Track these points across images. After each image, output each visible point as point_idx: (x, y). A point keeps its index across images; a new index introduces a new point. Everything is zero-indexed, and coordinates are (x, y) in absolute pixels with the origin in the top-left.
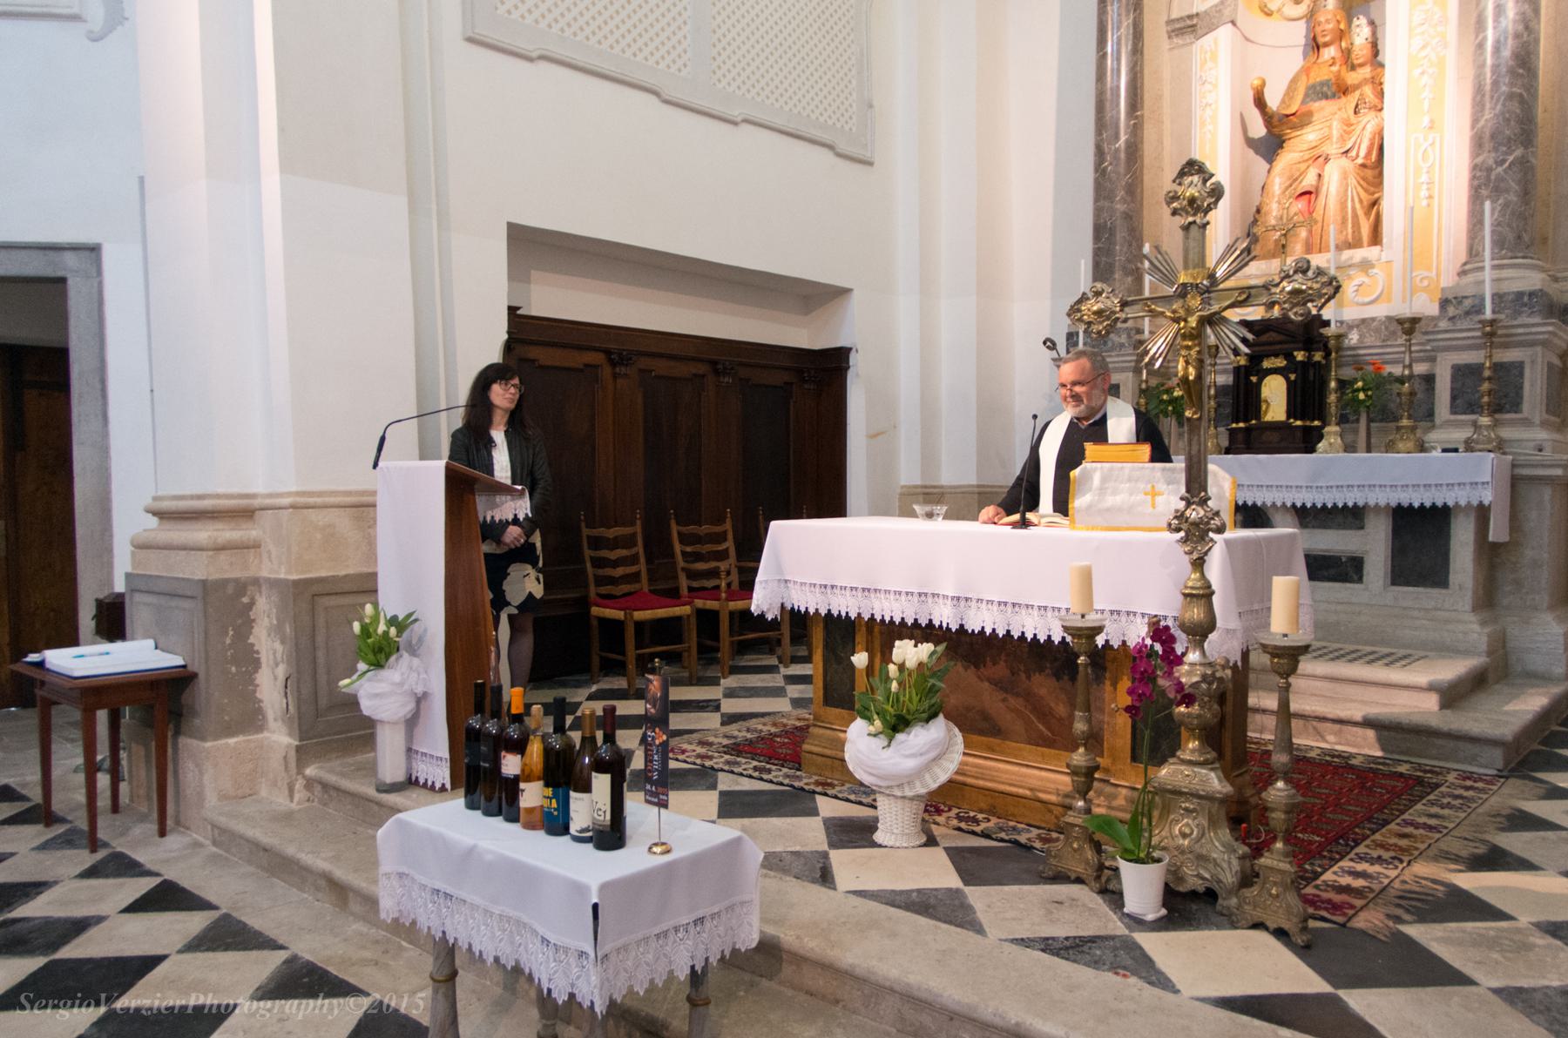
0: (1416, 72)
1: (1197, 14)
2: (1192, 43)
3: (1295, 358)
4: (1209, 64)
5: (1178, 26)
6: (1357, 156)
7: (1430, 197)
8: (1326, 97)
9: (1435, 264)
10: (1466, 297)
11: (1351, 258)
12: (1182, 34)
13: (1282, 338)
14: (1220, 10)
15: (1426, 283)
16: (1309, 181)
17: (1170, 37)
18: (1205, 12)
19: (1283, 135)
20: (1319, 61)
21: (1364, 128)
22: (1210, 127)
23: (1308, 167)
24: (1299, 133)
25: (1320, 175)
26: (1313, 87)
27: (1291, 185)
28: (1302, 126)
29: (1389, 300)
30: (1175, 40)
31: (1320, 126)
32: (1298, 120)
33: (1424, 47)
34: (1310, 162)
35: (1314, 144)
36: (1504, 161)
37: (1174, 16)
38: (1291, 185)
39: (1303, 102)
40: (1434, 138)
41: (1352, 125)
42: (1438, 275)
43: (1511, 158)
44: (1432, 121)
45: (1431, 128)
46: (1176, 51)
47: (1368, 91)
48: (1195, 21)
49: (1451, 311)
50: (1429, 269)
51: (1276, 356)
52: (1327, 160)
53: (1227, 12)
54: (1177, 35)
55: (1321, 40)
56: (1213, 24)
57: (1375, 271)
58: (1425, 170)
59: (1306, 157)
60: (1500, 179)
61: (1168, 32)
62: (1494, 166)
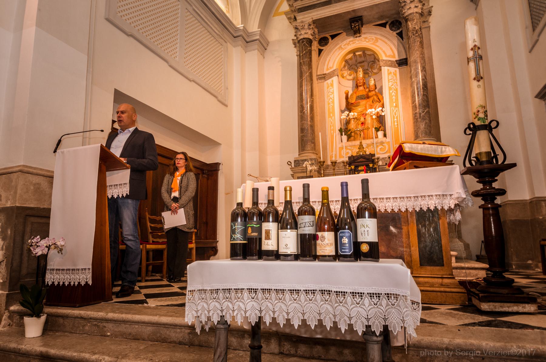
0: (391, 91)
3: (369, 166)
4: (330, 87)
5: (320, 77)
8: (363, 99)
13: (365, 160)
17: (317, 80)
18: (328, 73)
22: (332, 104)
25: (365, 119)
26: (358, 96)
28: (357, 106)
31: (363, 106)
32: (356, 105)
33: (392, 85)
35: (361, 111)
36: (424, 112)
37: (318, 74)
39: (356, 100)
43: (426, 111)
44: (396, 105)
46: (319, 84)
47: (376, 98)
51: (363, 166)
53: (336, 73)
55: (359, 84)
59: (360, 114)
60: (424, 116)
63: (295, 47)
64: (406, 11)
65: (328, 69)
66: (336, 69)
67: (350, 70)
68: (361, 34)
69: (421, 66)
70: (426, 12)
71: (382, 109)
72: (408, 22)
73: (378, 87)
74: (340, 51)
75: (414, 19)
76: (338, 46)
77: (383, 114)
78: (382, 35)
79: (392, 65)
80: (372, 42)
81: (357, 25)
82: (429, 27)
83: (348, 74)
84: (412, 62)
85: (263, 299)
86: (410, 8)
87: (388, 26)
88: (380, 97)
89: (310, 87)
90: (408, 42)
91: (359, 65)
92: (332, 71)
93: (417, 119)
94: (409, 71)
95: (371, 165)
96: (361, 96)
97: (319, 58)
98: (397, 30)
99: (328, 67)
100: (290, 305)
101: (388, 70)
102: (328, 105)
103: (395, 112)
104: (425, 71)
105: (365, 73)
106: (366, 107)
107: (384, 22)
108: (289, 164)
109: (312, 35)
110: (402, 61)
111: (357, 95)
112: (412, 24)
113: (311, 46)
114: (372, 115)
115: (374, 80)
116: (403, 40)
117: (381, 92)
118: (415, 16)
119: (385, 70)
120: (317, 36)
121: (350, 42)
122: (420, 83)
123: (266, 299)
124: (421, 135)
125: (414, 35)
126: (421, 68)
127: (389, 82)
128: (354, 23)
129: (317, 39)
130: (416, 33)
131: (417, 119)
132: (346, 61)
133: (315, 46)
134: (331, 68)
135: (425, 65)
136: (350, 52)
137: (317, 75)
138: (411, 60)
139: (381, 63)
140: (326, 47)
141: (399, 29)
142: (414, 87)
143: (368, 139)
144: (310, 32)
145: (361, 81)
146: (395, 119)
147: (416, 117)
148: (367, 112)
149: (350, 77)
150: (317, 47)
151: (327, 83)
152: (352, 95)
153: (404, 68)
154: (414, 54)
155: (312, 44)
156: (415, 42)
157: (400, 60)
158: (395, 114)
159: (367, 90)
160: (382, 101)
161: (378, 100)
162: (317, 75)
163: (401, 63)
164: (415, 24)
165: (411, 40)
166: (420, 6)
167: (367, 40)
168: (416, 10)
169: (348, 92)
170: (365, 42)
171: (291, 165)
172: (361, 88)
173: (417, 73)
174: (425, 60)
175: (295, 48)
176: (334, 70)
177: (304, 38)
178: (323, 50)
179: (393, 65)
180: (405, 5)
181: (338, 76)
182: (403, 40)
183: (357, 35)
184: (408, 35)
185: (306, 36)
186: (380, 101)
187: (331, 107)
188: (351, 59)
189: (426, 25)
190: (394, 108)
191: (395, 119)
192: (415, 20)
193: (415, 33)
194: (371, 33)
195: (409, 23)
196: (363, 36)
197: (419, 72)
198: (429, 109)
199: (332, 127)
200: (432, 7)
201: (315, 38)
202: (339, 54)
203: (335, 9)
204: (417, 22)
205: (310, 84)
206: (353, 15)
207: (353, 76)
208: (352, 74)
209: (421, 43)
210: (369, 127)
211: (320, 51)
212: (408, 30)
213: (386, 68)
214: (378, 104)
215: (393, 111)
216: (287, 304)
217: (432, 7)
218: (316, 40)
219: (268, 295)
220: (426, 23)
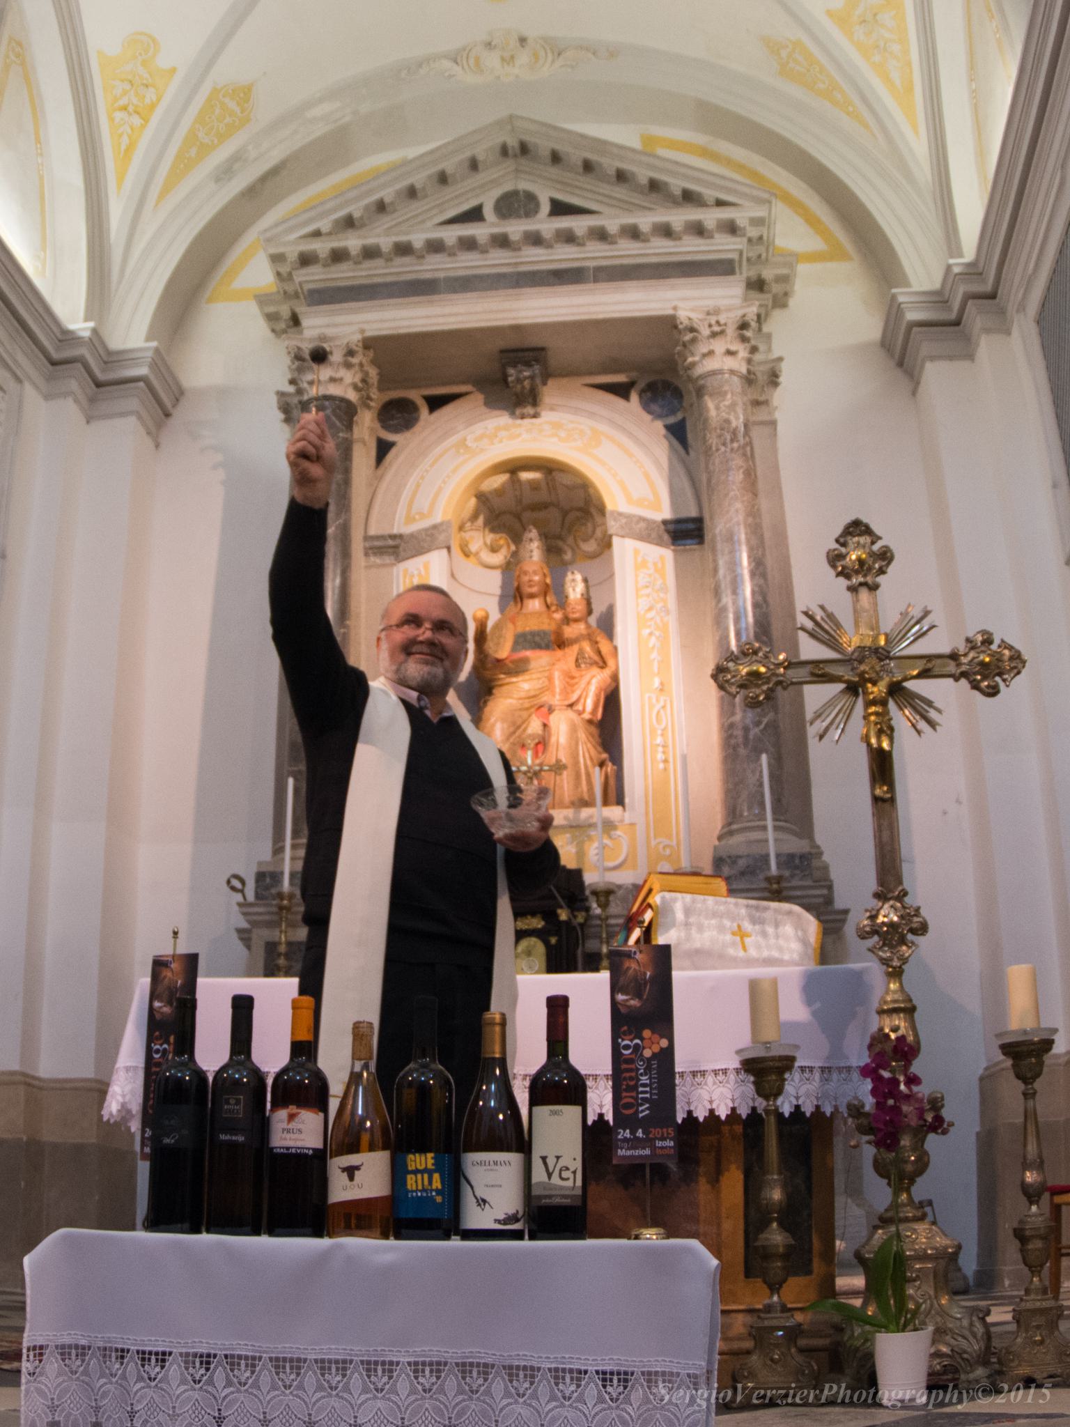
0: (646, 632)
1: (400, 536)
2: (393, 565)
3: (556, 916)
6: (584, 710)
7: (666, 761)
9: (674, 832)
10: (740, 857)
11: (591, 817)
15: (668, 852)
16: (535, 726)
17: (366, 554)
18: (412, 536)
20: (524, 611)
21: (589, 683)
23: (530, 716)
24: (514, 680)
25: (545, 725)
27: (514, 733)
29: (634, 867)
30: (372, 559)
33: (650, 609)
34: (533, 710)
35: (532, 693)
37: (372, 531)
38: (514, 733)
40: (665, 701)
42: (678, 844)
43: (765, 720)
44: (662, 684)
45: (662, 690)
48: (397, 542)
49: (726, 870)
50: (669, 837)
51: (533, 914)
52: (551, 710)
53: (442, 537)
54: (375, 554)
55: (527, 590)
57: (618, 833)
58: (659, 732)
59: (527, 705)
61: (365, 548)
62: (751, 726)
64: (697, 358)
65: (410, 519)
66: (441, 524)
67: (493, 530)
68: (539, 409)
69: (749, 557)
70: (761, 371)
72: (706, 398)
73: (597, 608)
75: (726, 393)
76: (453, 439)
78: (611, 422)
79: (649, 535)
81: (526, 378)
82: (773, 424)
83: (485, 544)
84: (719, 538)
85: (274, 1387)
86: (711, 353)
87: (634, 397)
88: (605, 647)
89: (338, 581)
90: (707, 467)
91: (527, 515)
92: (426, 530)
93: (735, 748)
94: (711, 566)
95: (563, 915)
96: (533, 634)
97: (380, 471)
98: (667, 416)
99: (414, 511)
100: (361, 1405)
101: (636, 552)
103: (658, 712)
104: (764, 575)
105: (553, 550)
107: (621, 378)
108: (233, 889)
109: (356, 387)
110: (684, 526)
111: (520, 630)
112: (717, 408)
113: (349, 426)
115: (585, 580)
116: (688, 453)
117: (607, 625)
118: (727, 381)
119: (626, 551)
120: (374, 393)
121: (498, 429)
122: (746, 617)
123: (285, 1387)
124: (750, 808)
125: (724, 444)
126: (749, 563)
127: (637, 596)
128: (515, 367)
129: (372, 404)
130: (732, 441)
131: (735, 748)
132: (482, 498)
133: (366, 426)
134: (423, 516)
135: (764, 555)
136: (498, 468)
137: (367, 538)
138: (717, 528)
139: (612, 526)
140: (408, 434)
141: (673, 412)
142: (727, 629)
144: (349, 377)
145: (536, 578)
147: (733, 741)
149: (495, 555)
150: (372, 429)
151: (406, 571)
152: (498, 626)
153: (691, 546)
154: (728, 512)
155: (355, 419)
156: (728, 470)
157: (678, 521)
158: (658, 720)
159: (558, 616)
160: (611, 662)
161: (596, 658)
162: (367, 538)
163: (682, 532)
164: (728, 407)
165: (717, 460)
166: (743, 353)
167: (563, 434)
168: (730, 363)
169: (487, 617)
170: (555, 439)
171: (242, 891)
172: (535, 605)
173: (736, 576)
174: (762, 535)
176: (435, 527)
177: (327, 398)
179: (654, 535)
180: (694, 340)
181: (449, 548)
182: (688, 453)
185: (334, 390)
186: (604, 662)
188: (499, 492)
189: (761, 415)
191: (659, 740)
192: (729, 396)
193: (728, 437)
194: (576, 411)
195: (710, 403)
196: (547, 416)
197: (742, 575)
198: (776, 713)
200: (780, 359)
201: (369, 398)
202: (454, 471)
203: (447, 310)
204: (733, 406)
205: (339, 571)
206: (513, 342)
207: (504, 551)
208: (501, 547)
209: (750, 475)
210: (564, 761)
211: (383, 449)
215: (651, 706)
216: (353, 1402)
217: (780, 359)
218: (368, 407)
219: (293, 1377)
220: (763, 407)
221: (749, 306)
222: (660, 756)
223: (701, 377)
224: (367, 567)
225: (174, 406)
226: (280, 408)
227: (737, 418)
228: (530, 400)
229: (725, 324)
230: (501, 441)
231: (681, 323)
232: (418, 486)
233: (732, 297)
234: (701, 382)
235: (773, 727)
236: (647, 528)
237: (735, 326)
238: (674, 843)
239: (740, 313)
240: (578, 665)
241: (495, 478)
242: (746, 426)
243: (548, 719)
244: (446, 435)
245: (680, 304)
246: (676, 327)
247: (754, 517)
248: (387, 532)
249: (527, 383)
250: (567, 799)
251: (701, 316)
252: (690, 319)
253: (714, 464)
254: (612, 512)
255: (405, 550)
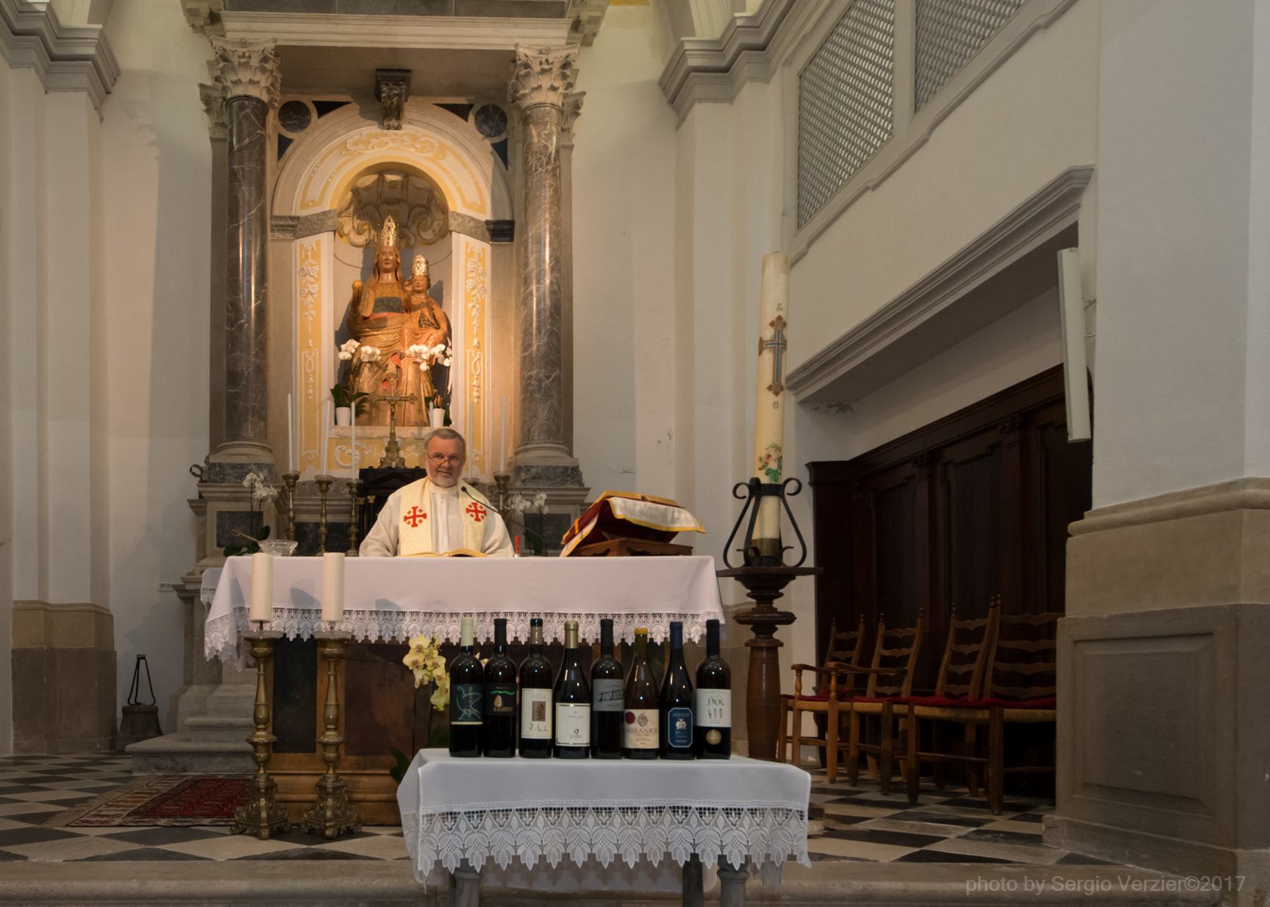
1: (298, 218)
4: (310, 260)
5: (281, 223)
7: (478, 397)
12: (283, 231)
14: (323, 219)
15: (477, 459)
18: (306, 218)
19: (362, 332)
24: (376, 333)
25: (398, 367)
30: (277, 234)
35: (388, 344)
41: (418, 334)
42: (484, 454)
44: (478, 343)
50: (480, 450)
54: (279, 230)
56: (315, 229)
59: (386, 352)
63: (208, 111)
64: (527, 92)
65: (304, 205)
66: (331, 211)
71: (446, 349)
72: (531, 126)
74: (344, 159)
75: (547, 122)
77: (446, 363)
79: (476, 232)
80: (430, 154)
84: (530, 240)
86: (540, 87)
90: (526, 183)
92: (318, 215)
99: (307, 199)
101: (467, 244)
102: (301, 313)
103: (475, 363)
104: (559, 270)
106: (401, 334)
112: (539, 135)
114: (418, 360)
118: (548, 113)
125: (541, 166)
130: (548, 164)
134: (315, 204)
139: (453, 224)
143: (404, 426)
146: (475, 382)
148: (407, 352)
150: (275, 127)
158: (475, 369)
159: (409, 289)
160: (443, 325)
170: (412, 150)
173: (540, 271)
175: (205, 115)
176: (324, 213)
178: (291, 141)
180: (527, 75)
183: (391, 123)
184: (526, 162)
187: (310, 318)
190: (473, 352)
191: (475, 382)
199: (311, 380)
202: (340, 167)
211: (284, 144)
212: (527, 148)
213: (462, 236)
214: (437, 334)
215: (471, 360)
221: (572, 48)
222: (475, 394)
223: (528, 108)
224: (273, 240)
225: (113, 85)
226: (202, 100)
227: (552, 145)
228: (395, 115)
229: (552, 63)
230: (373, 148)
231: (520, 60)
232: (311, 178)
233: (560, 38)
234: (529, 112)
235: (558, 379)
236: (475, 227)
237: (559, 66)
238: (482, 453)
239: (565, 53)
240: (421, 326)
241: (369, 177)
242: (557, 151)
243: (400, 363)
244: (331, 137)
245: (521, 42)
246: (514, 61)
247: (557, 226)
248: (287, 214)
249: (395, 100)
250: (413, 420)
251: (535, 54)
252: (526, 56)
253: (532, 182)
254: (453, 212)
255: (300, 230)
